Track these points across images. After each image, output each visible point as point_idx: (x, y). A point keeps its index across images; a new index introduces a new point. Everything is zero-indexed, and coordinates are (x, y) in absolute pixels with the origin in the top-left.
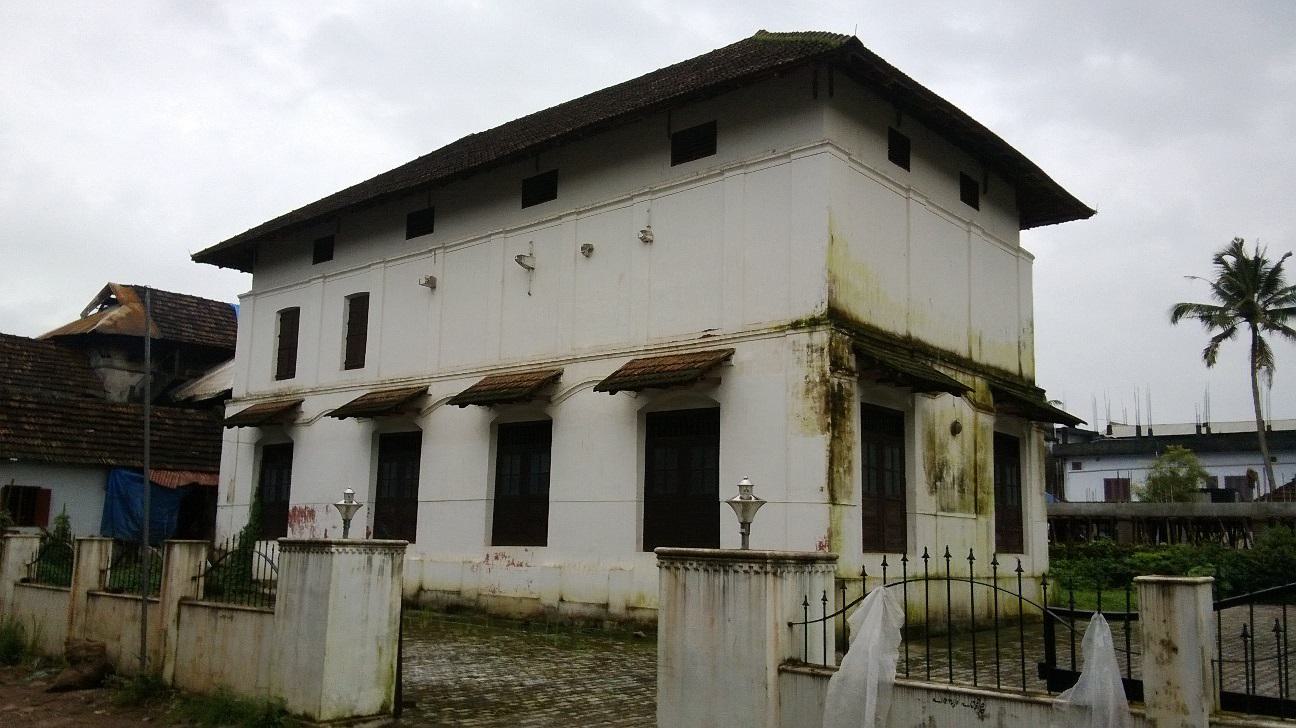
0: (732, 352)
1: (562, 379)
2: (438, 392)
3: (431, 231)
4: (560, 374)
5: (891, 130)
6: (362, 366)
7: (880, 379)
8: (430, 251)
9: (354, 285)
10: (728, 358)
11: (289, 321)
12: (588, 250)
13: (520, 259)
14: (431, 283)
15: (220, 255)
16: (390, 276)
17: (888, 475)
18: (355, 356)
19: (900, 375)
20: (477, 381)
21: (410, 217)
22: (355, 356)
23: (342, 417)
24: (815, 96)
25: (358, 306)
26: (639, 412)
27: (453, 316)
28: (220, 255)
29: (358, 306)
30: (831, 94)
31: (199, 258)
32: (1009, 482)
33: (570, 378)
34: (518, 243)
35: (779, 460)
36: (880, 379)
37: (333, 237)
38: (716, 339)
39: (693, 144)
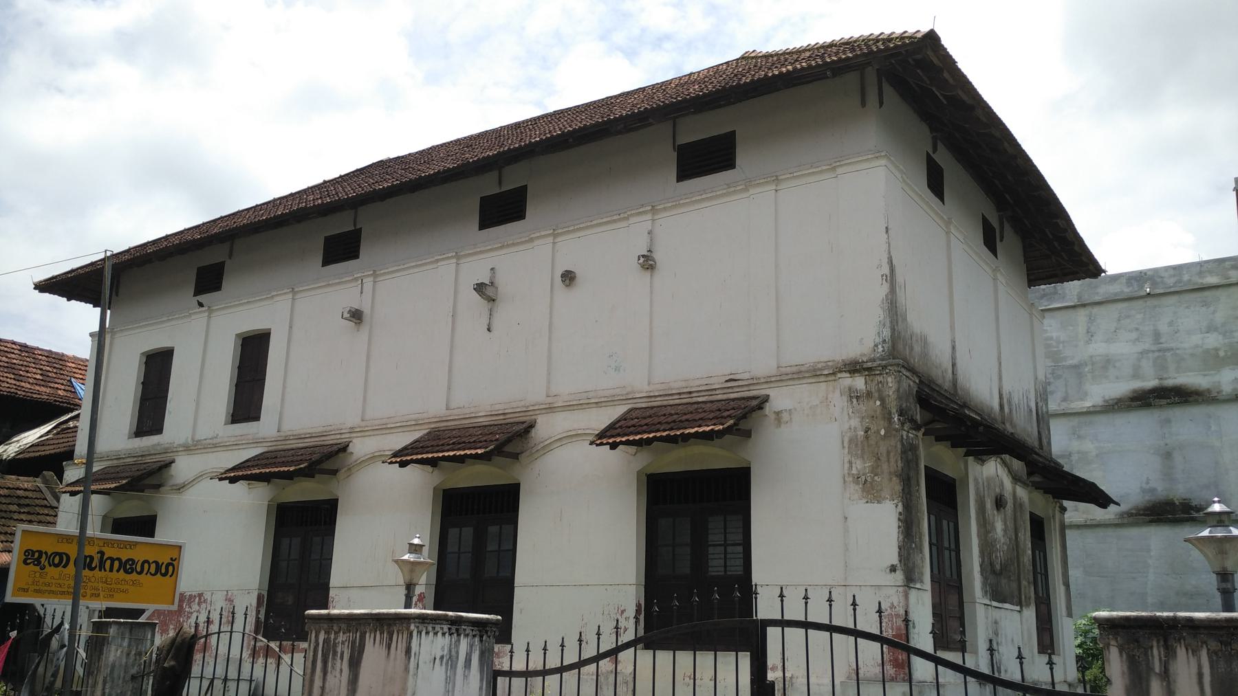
0: (766, 399)
1: (533, 432)
2: (361, 448)
3: (356, 256)
4: (532, 426)
5: (929, 157)
6: (257, 418)
7: (940, 438)
8: (356, 279)
9: (250, 319)
10: (760, 407)
11: (158, 366)
12: (569, 278)
13: (480, 288)
14: (356, 316)
15: (72, 285)
16: (301, 313)
17: (947, 553)
18: (246, 401)
19: (981, 429)
20: (417, 435)
21: (328, 240)
22: (246, 401)
23: (233, 480)
24: (863, 104)
25: (253, 350)
26: (639, 473)
27: (374, 362)
28: (72, 285)
29: (253, 350)
30: (881, 104)
31: (46, 286)
32: (946, 544)
33: (547, 427)
34: (476, 269)
35: (824, 537)
36: (940, 438)
37: (222, 265)
38: (740, 383)
39: (706, 159)
